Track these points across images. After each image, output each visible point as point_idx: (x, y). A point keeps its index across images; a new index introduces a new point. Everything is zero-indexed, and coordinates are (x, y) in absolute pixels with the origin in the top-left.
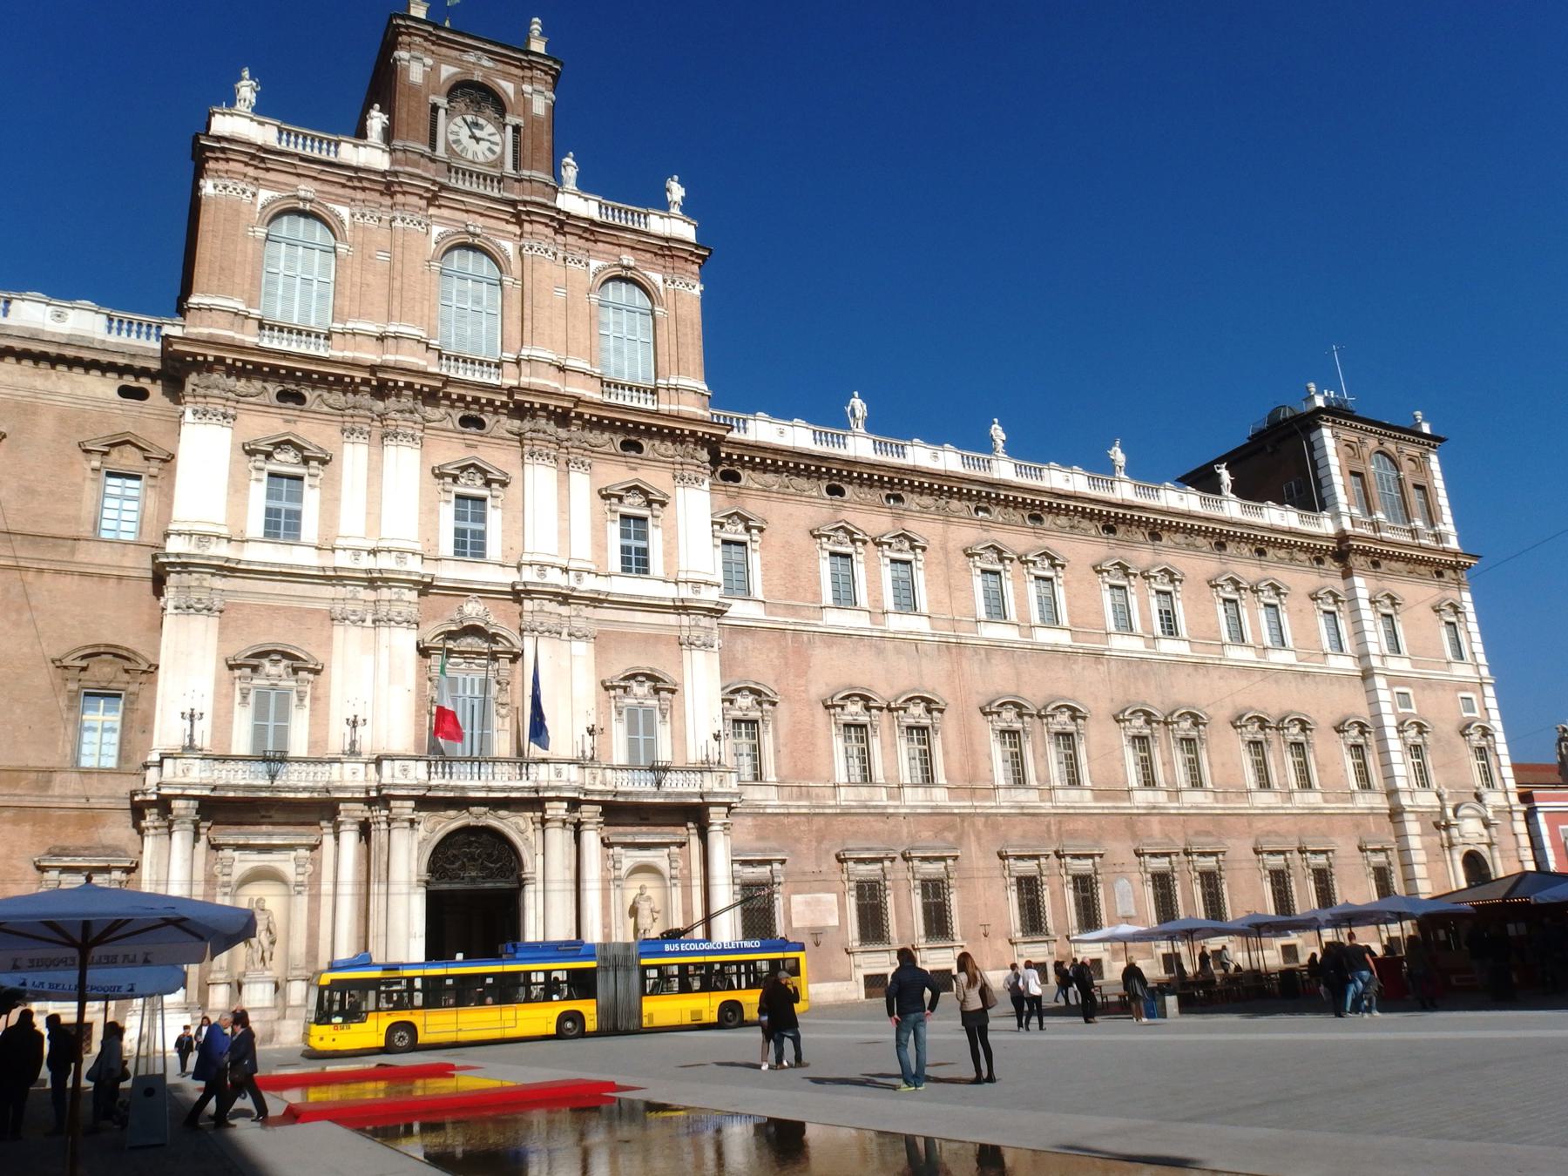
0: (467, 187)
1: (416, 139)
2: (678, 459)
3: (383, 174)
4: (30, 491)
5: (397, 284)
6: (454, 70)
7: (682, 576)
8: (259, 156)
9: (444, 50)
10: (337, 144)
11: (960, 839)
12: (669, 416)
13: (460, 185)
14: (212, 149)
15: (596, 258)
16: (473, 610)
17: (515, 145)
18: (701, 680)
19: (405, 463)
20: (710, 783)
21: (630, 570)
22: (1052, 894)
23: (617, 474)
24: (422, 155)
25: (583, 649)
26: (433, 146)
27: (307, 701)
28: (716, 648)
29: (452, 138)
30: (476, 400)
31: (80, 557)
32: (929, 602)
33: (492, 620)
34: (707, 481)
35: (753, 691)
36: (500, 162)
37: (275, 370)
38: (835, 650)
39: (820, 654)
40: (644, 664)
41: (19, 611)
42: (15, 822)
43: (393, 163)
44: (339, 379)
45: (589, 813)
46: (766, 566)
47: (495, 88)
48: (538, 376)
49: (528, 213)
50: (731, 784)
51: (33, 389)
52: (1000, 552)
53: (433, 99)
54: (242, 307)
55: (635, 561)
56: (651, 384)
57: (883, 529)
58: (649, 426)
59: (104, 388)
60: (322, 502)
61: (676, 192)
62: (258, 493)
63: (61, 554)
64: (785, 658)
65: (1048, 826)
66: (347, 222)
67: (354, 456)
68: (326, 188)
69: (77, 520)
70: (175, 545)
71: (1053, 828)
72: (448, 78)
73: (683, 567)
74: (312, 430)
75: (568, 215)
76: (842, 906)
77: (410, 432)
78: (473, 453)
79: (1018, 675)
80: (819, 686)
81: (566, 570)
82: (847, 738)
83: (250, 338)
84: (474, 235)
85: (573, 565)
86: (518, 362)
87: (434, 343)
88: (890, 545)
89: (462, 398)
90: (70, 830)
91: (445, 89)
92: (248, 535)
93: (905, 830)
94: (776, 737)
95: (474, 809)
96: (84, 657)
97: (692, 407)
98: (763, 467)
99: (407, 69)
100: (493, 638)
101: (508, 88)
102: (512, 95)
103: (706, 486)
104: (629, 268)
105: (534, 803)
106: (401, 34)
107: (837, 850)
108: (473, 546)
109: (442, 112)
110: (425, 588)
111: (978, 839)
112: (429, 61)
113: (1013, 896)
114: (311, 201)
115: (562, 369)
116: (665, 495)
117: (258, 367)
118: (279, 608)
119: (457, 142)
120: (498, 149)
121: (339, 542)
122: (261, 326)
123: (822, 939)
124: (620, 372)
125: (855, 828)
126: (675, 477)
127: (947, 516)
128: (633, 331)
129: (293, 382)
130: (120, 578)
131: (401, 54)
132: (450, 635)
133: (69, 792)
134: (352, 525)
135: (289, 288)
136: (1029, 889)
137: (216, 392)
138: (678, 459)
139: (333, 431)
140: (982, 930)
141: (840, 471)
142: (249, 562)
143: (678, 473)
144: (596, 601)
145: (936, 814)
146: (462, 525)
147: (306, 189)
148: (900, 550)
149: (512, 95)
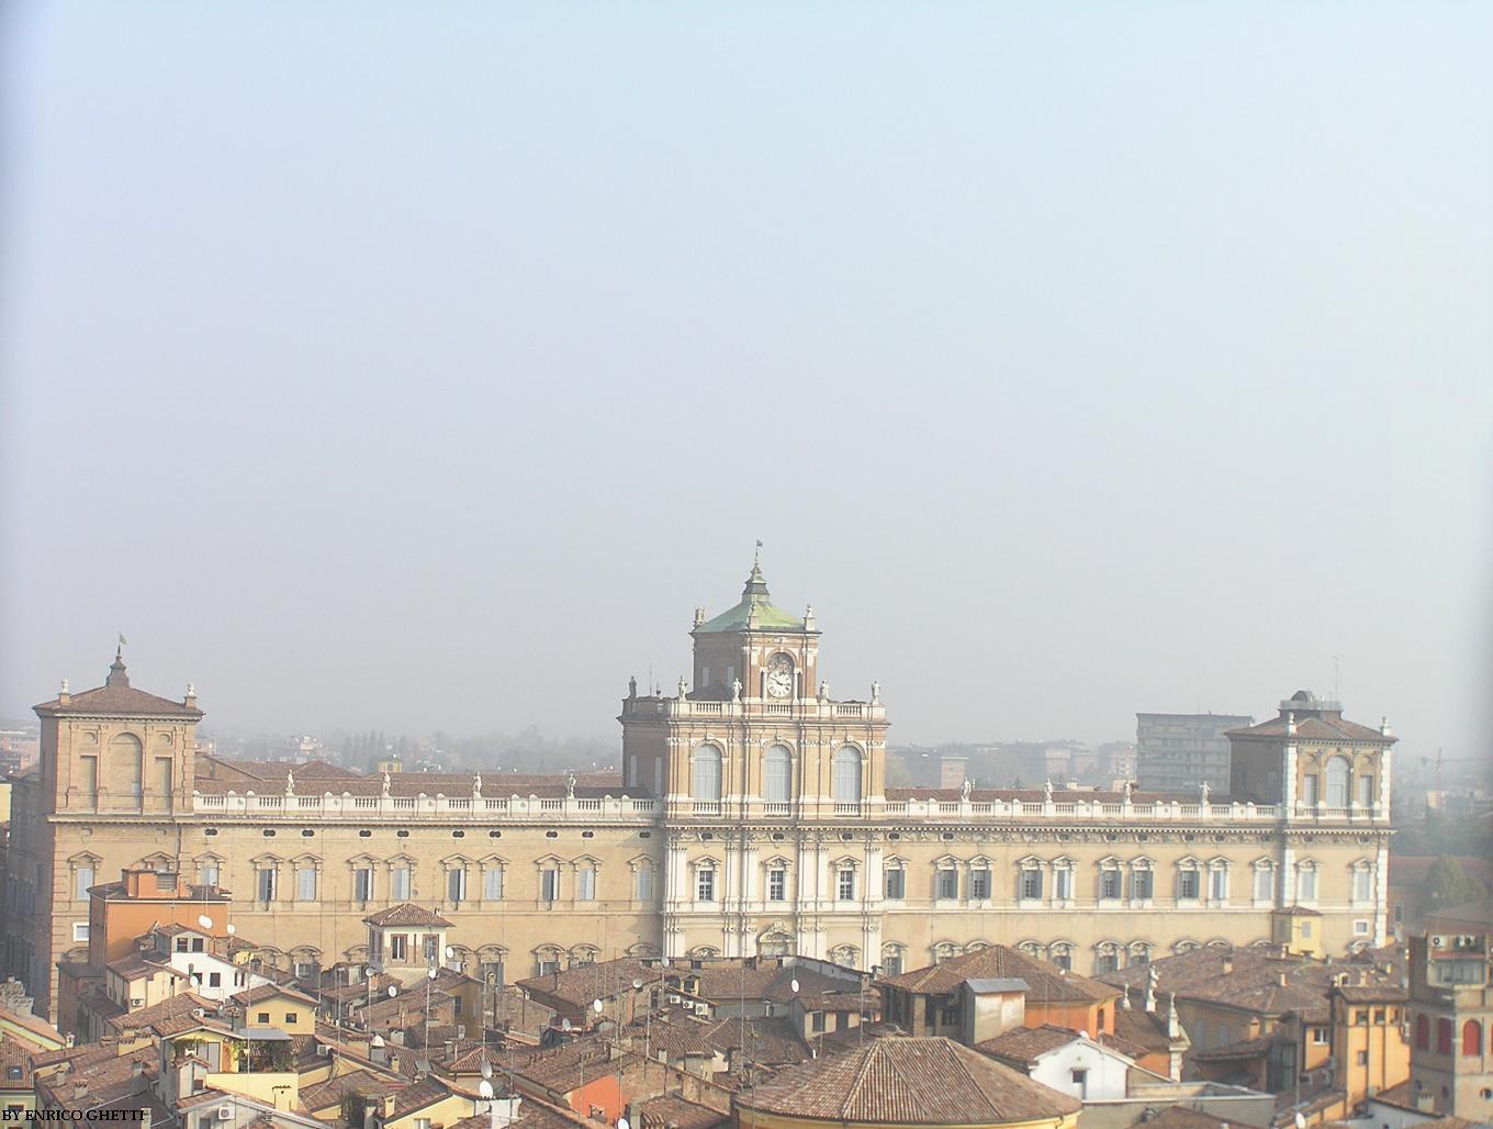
8: (691, 721)
10: (721, 705)
16: (779, 925)
19: (753, 860)
26: (761, 697)
36: (792, 696)
53: (761, 669)
57: (972, 855)
80: (927, 942)
101: (796, 651)
109: (765, 675)
119: (772, 688)
146: (773, 883)
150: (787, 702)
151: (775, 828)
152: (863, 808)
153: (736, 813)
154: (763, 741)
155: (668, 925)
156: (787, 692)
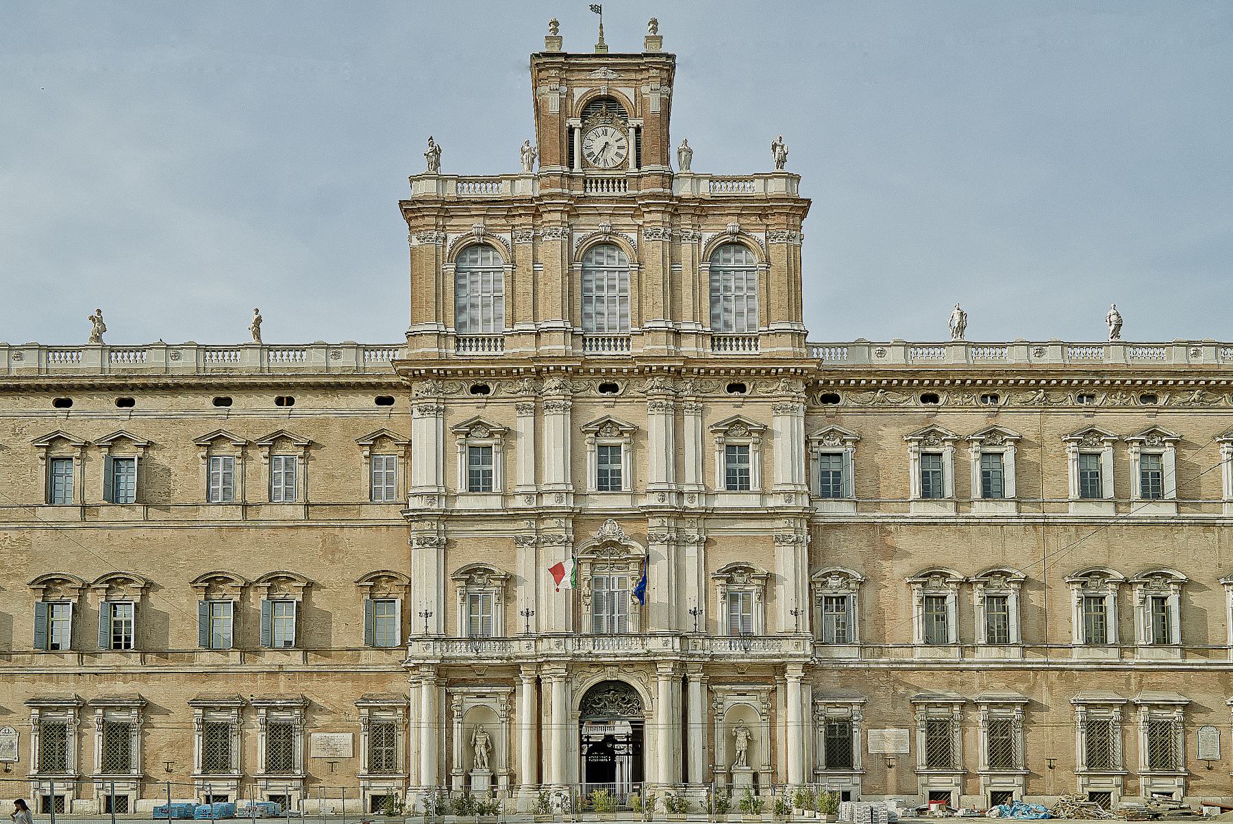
9: (576, 76)
11: (1031, 689)
13: (594, 193)
14: (412, 211)
16: (609, 529)
17: (638, 144)
23: (722, 411)
26: (571, 166)
29: (586, 152)
35: (840, 574)
36: (623, 165)
37: (466, 372)
43: (543, 186)
44: (509, 372)
49: (647, 205)
58: (748, 372)
67: (524, 425)
70: (415, 503)
72: (580, 100)
74: (495, 413)
76: (913, 739)
78: (610, 412)
79: (1110, 548)
82: (928, 609)
87: (578, 330)
89: (598, 371)
91: (579, 110)
93: (977, 681)
98: (858, 388)
99: (546, 102)
103: (802, 414)
105: (650, 664)
109: (577, 132)
112: (564, 89)
113: (1080, 740)
115: (677, 333)
117: (455, 372)
121: (520, 490)
131: (543, 89)
134: (523, 475)
136: (1097, 734)
139: (511, 409)
140: (1047, 763)
141: (932, 382)
142: (459, 511)
144: (708, 514)
145: (1008, 668)
151: (598, 371)
154: (577, 235)
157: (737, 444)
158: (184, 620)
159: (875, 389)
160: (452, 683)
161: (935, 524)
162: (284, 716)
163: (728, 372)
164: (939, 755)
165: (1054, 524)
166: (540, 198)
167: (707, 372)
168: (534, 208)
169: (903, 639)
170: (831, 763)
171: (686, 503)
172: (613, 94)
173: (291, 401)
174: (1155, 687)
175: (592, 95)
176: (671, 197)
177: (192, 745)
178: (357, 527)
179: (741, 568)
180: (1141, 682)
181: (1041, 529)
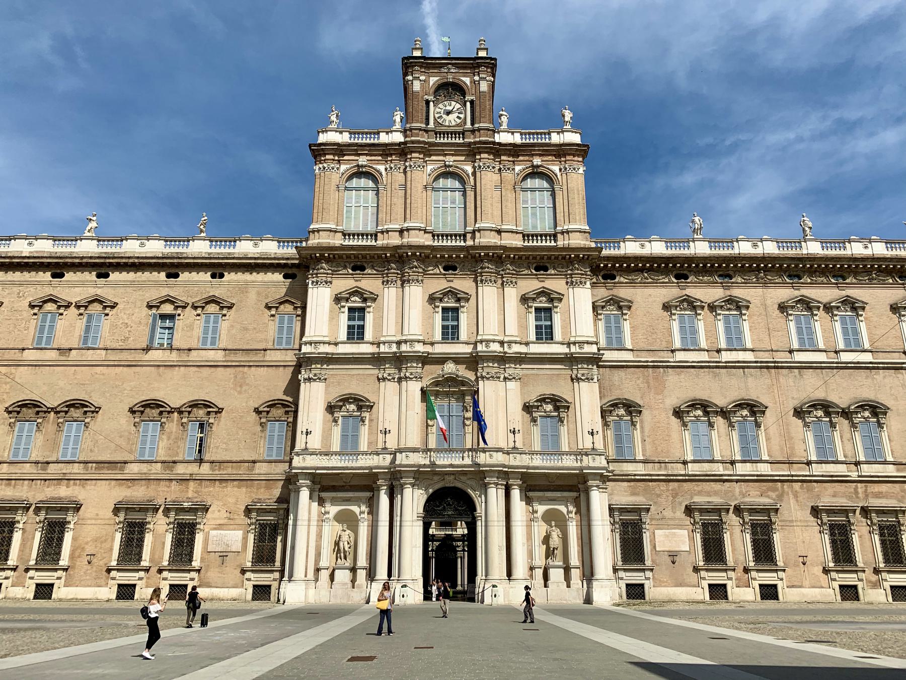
0: (446, 141)
1: (417, 122)
2: (569, 272)
3: (400, 144)
4: (246, 329)
5: (408, 201)
6: (436, 79)
7: (572, 339)
11: (780, 497)
12: (564, 249)
13: (442, 141)
15: (519, 165)
16: (450, 367)
18: (587, 400)
19: (416, 294)
20: (587, 461)
21: (542, 339)
22: (860, 537)
23: (530, 285)
24: (420, 130)
25: (511, 385)
26: (427, 123)
27: (367, 422)
28: (595, 380)
29: (437, 116)
30: (450, 257)
31: (267, 358)
32: (753, 340)
33: (460, 373)
34: (588, 283)
37: (348, 256)
38: (683, 376)
39: (672, 377)
40: (548, 391)
41: (241, 386)
42: (239, 487)
43: (406, 137)
44: (379, 257)
45: (515, 482)
46: (633, 328)
47: (460, 83)
48: (485, 237)
50: (601, 462)
51: (246, 281)
52: (808, 303)
54: (333, 226)
55: (545, 334)
56: (552, 231)
58: (549, 258)
59: (278, 277)
60: (374, 320)
61: (568, 115)
62: (344, 317)
63: (259, 357)
64: (648, 382)
65: (856, 489)
66: (384, 173)
68: (373, 158)
69: (266, 340)
70: (305, 349)
71: (860, 490)
73: (573, 334)
74: (370, 284)
75: (499, 144)
76: (692, 539)
77: (415, 278)
78: (451, 284)
81: (502, 343)
83: (337, 241)
84: (450, 166)
85: (506, 339)
86: (474, 232)
88: (722, 307)
90: (262, 490)
91: (432, 91)
92: (339, 340)
93: (737, 490)
94: (642, 432)
95: (446, 477)
96: (268, 407)
97: (577, 241)
98: (628, 271)
100: (463, 383)
101: (467, 80)
102: (468, 83)
103: (588, 285)
104: (538, 166)
105: (480, 476)
106: (408, 67)
107: (687, 503)
108: (453, 333)
109: (431, 104)
110: (426, 360)
111: (796, 496)
114: (366, 166)
115: (499, 232)
116: (560, 294)
117: (340, 257)
118: (353, 375)
120: (462, 116)
121: (382, 339)
122: (344, 235)
123: (677, 559)
124: (535, 227)
125: (700, 488)
126: (567, 283)
127: (765, 285)
128: (542, 201)
129: (357, 260)
130: (285, 366)
131: (410, 78)
132: (437, 383)
133: (262, 472)
135: (357, 213)
137: (322, 271)
138: (569, 272)
140: (801, 559)
143: (569, 280)
144: (521, 359)
145: (760, 479)
146: (446, 323)
147: (363, 160)
148: (729, 309)
149: (468, 83)
150: (460, 129)
151: (443, 257)
152: (559, 236)
153: (394, 240)
154: (430, 167)
155: (304, 375)
156: (459, 121)
157: (544, 308)
158: (121, 437)
159: (642, 270)
160: (324, 489)
161: (693, 367)
162: (188, 517)
163: (535, 258)
164: (714, 551)
165: (782, 368)
166: (405, 143)
167: (520, 258)
168: (402, 151)
169: (677, 455)
170: (626, 559)
171: (506, 349)
172: (456, 81)
173: (222, 276)
174: (878, 495)
175: (442, 81)
176: (494, 143)
177: (113, 540)
178: (261, 366)
179: (548, 398)
180: (866, 490)
181: (773, 370)
